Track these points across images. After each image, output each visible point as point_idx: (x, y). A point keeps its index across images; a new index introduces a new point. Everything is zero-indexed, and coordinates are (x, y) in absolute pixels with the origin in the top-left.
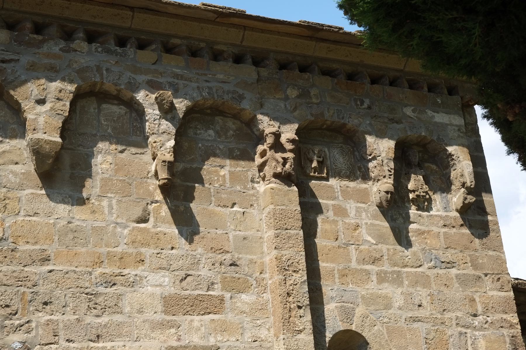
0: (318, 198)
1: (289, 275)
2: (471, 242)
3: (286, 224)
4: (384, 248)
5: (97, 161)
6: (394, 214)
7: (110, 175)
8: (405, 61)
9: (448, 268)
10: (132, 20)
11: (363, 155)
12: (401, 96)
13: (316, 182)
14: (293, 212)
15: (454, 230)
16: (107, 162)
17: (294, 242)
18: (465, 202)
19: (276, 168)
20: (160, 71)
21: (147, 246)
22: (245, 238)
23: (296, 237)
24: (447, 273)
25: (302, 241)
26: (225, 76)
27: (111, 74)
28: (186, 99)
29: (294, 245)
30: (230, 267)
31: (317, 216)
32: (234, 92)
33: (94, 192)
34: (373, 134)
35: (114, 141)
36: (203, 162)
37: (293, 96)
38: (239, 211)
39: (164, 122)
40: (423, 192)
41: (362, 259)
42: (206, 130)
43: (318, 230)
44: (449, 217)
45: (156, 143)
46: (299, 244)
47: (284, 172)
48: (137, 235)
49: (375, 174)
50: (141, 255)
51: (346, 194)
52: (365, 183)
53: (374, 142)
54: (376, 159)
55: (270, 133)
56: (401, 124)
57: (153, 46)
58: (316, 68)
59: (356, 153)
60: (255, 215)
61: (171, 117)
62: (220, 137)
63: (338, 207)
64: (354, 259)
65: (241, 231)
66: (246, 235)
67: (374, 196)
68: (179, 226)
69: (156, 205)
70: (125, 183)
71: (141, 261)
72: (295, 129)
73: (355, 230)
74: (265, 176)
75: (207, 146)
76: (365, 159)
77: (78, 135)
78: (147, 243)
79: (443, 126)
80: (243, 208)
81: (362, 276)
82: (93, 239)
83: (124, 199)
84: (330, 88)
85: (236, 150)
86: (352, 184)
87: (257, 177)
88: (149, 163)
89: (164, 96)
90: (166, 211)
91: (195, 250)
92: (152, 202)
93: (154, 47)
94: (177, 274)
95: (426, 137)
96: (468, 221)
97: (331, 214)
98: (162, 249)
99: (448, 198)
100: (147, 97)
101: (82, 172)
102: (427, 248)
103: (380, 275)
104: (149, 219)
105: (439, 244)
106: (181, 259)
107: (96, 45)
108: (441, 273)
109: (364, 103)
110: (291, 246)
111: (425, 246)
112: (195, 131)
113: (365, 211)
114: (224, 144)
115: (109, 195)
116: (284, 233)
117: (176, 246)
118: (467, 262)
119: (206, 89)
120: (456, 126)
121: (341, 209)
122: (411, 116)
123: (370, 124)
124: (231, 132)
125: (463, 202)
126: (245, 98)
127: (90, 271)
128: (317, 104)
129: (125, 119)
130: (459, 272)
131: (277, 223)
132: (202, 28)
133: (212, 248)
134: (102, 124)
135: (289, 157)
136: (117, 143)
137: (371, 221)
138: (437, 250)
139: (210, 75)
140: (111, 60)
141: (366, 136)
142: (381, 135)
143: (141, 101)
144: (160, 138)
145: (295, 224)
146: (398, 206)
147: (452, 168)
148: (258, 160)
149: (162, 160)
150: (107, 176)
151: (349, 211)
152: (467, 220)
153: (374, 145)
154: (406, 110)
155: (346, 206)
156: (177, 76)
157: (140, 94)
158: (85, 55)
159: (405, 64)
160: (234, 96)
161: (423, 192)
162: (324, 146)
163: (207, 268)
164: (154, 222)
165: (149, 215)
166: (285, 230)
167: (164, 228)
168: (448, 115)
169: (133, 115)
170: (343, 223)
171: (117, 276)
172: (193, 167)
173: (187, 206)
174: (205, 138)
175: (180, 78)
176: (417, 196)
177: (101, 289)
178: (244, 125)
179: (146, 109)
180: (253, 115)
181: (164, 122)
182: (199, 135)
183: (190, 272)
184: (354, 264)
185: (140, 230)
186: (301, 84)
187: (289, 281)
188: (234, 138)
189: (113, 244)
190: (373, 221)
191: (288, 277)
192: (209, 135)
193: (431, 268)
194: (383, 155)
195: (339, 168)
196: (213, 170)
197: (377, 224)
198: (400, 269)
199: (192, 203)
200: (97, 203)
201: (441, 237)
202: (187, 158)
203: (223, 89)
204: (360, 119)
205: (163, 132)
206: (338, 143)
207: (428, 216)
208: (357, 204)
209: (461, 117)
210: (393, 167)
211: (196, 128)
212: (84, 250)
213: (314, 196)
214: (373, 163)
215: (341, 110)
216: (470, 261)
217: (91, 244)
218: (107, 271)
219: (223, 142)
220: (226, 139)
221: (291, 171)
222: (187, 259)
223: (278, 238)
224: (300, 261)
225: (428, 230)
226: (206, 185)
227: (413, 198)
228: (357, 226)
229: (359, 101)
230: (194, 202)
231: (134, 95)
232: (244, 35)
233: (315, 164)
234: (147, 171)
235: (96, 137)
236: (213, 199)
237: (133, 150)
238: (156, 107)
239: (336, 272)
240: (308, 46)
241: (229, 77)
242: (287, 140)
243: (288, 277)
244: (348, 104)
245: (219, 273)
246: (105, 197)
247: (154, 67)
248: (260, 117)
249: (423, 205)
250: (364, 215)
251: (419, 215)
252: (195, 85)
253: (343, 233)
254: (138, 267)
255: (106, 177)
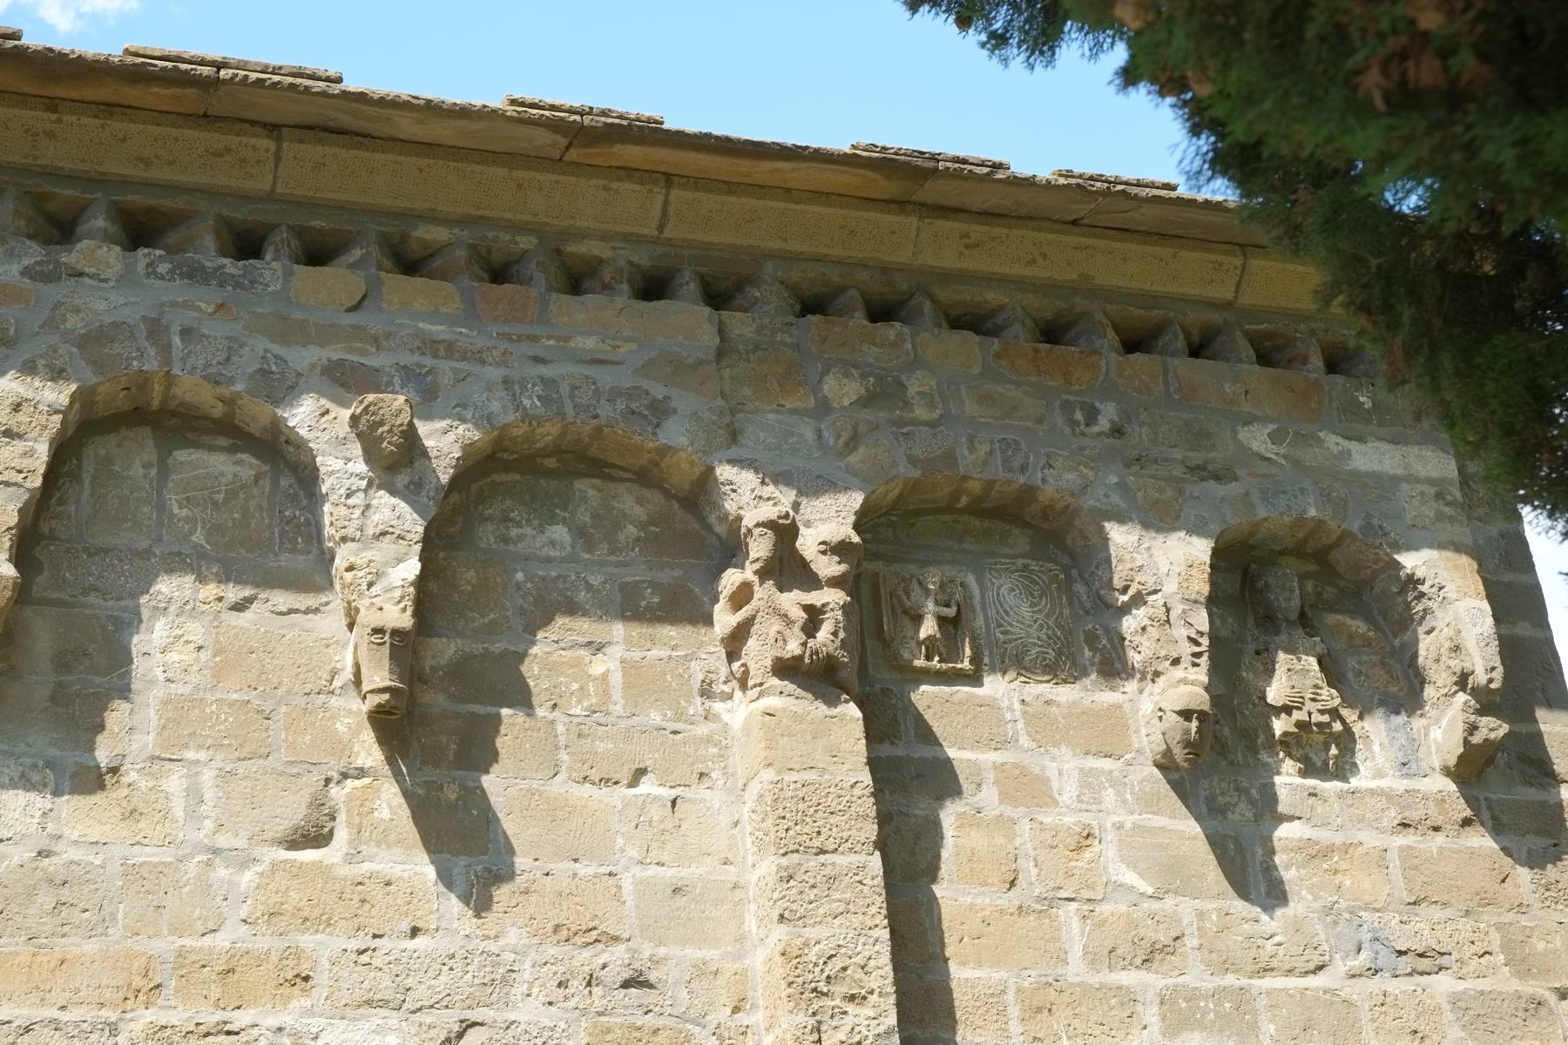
0: (944, 743)
1: (830, 1012)
2: (1503, 881)
3: (819, 833)
4: (1184, 909)
5: (150, 641)
6: (1218, 791)
7: (197, 688)
8: (1238, 272)
9: (1422, 973)
10: (276, 167)
11: (1102, 592)
12: (1227, 390)
13: (936, 689)
14: (843, 793)
15: (1440, 839)
16: (187, 642)
17: (848, 896)
18: (1470, 738)
19: (780, 643)
20: (373, 332)
21: (321, 927)
22: (680, 889)
23: (857, 878)
24: (1420, 991)
25: (878, 890)
26: (604, 342)
27: (199, 347)
28: (463, 420)
29: (851, 906)
30: (623, 991)
31: (941, 807)
32: (633, 393)
33: (135, 746)
34: (1131, 520)
35: (215, 570)
36: (530, 634)
37: (846, 402)
38: (656, 797)
39: (383, 499)
40: (1322, 712)
41: (1106, 951)
42: (541, 525)
43: (945, 854)
44: (1420, 797)
45: (353, 572)
46: (869, 901)
47: (811, 655)
48: (288, 888)
49: (1142, 653)
50: (299, 959)
51: (1043, 725)
52: (1113, 689)
53: (1136, 544)
54: (1145, 603)
55: (758, 525)
56: (1234, 483)
57: (353, 252)
58: (927, 306)
59: (1080, 588)
60: (717, 807)
61: (411, 482)
62: (590, 546)
63: (1017, 772)
64: (1076, 952)
65: (663, 865)
66: (682, 878)
67: (1144, 731)
68: (440, 853)
69: (358, 783)
70: (248, 712)
71: (298, 980)
72: (853, 511)
73: (1079, 848)
74: (746, 673)
75: (544, 579)
76: (1108, 606)
77: (85, 556)
78: (324, 918)
79: (1385, 485)
80: (671, 787)
81: (1106, 1008)
82: (127, 909)
83: (243, 767)
84: (976, 370)
85: (649, 591)
86: (1065, 694)
87: (723, 679)
88: (337, 643)
89: (381, 412)
90: (394, 803)
91: (496, 937)
92: (345, 776)
93: (356, 254)
94: (429, 1020)
95: (1324, 522)
96: (1490, 808)
97: (988, 797)
98: (375, 936)
99: (1415, 730)
100: (324, 419)
101: (97, 680)
102: (1343, 904)
103: (1175, 1003)
104: (331, 832)
105: (1387, 891)
106: (446, 968)
107: (149, 254)
108: (1397, 992)
109: (1100, 418)
110: (840, 910)
111: (1335, 898)
112: (504, 531)
113: (1114, 783)
114: (604, 569)
115: (191, 755)
116: (812, 864)
117: (427, 922)
118: (1489, 950)
119: (534, 385)
120: (1430, 482)
121: (1025, 780)
122: (1268, 455)
123: (1122, 486)
124: (632, 530)
125: (1466, 742)
126: (675, 411)
127: (113, 1019)
128: (932, 424)
129: (253, 497)
130: (1461, 986)
131: (787, 830)
132: (519, 186)
133: (557, 928)
134: (171, 516)
135: (828, 603)
136: (224, 578)
137: (1136, 817)
138: (1376, 910)
139: (549, 338)
140: (201, 301)
141: (1108, 526)
142: (1159, 519)
143: (302, 432)
144: (368, 555)
145: (853, 832)
146: (1232, 763)
147: (1420, 624)
148: (725, 619)
149: (372, 626)
150: (187, 690)
151: (1055, 785)
152: (1483, 803)
153: (1135, 555)
154: (1249, 435)
155: (1043, 769)
156: (431, 346)
157: (301, 409)
158: (113, 287)
159: (1238, 284)
160: (633, 406)
161: (1322, 712)
162: (964, 568)
163: (541, 998)
164: (350, 843)
165: (334, 819)
166: (816, 854)
167: (387, 863)
168: (1399, 447)
169: (282, 483)
170: (1034, 826)
171: (212, 1034)
172: (492, 649)
173: (471, 784)
174: (538, 552)
175: (442, 352)
176: (1299, 724)
178: (676, 505)
179: (319, 459)
180: (702, 468)
181: (383, 501)
182: (515, 543)
183: (473, 1016)
184: (1076, 970)
185: (299, 870)
186: (871, 360)
187: (830, 1032)
188: (641, 550)
189: (199, 923)
190: (1144, 816)
191: (826, 1018)
192: (553, 543)
193: (1360, 975)
194: (1170, 587)
195: (1016, 639)
196: (563, 659)
197: (1160, 828)
198: (1244, 982)
199: (487, 772)
200: (144, 784)
201: (1391, 865)
202: (474, 621)
203: (594, 383)
204: (1085, 471)
205: (378, 531)
206: (1015, 557)
207: (1340, 796)
208: (1084, 762)
209: (1444, 451)
210: (1205, 627)
211: (506, 519)
212: (91, 947)
213: (927, 735)
214: (1135, 617)
215: (1016, 442)
216: (1501, 946)
217: (120, 926)
218: (173, 1018)
219: (602, 564)
220: (612, 552)
221: (836, 649)
222: (467, 969)
223: (792, 883)
224: (872, 963)
225: (1344, 844)
226: (541, 712)
227: (1285, 734)
228: (1085, 834)
229: (1082, 409)
230: (495, 769)
231: (279, 412)
232: (666, 203)
233: (928, 628)
234: (329, 668)
235: (149, 560)
236: (564, 756)
237: (281, 600)
238: (356, 449)
239: (1010, 997)
240: (893, 232)
241: (618, 343)
242: (823, 547)
243: (826, 1018)
244: (1040, 421)
245: (584, 1012)
246: (174, 760)
247: (353, 319)
248: (725, 472)
249: (1324, 756)
250: (1109, 796)
251: (1311, 791)
252: (494, 373)
253: (1035, 860)
254: (287, 1000)
255: (179, 692)
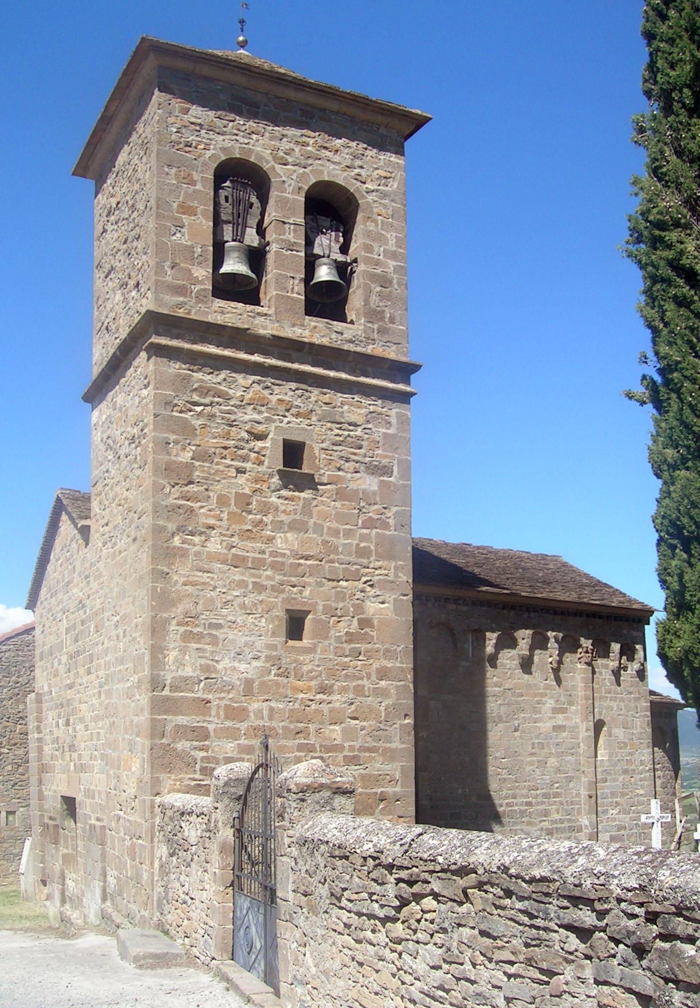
4: (612, 687)
79: (636, 637)
177: (537, 706)
